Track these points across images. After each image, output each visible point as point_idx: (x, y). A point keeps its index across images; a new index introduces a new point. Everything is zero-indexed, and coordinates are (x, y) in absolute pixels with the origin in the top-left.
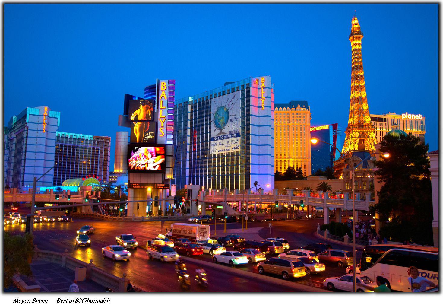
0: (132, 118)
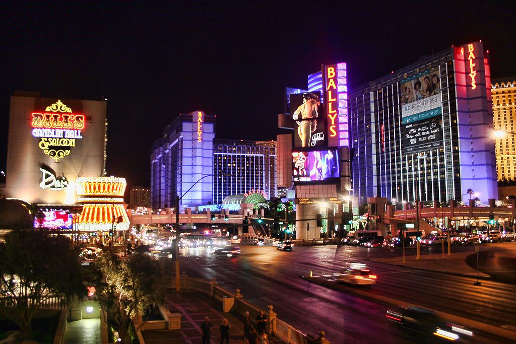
0: (295, 117)
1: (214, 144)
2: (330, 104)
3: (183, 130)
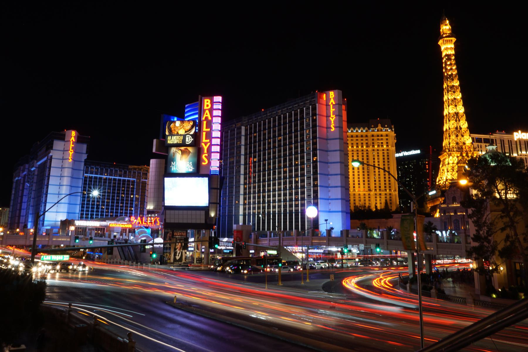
1: (85, 165)
2: (204, 133)
3: (54, 148)
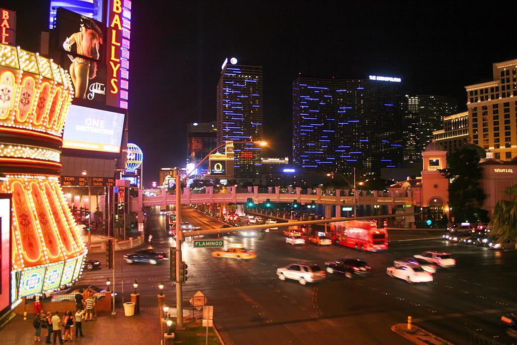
2: (113, 48)
